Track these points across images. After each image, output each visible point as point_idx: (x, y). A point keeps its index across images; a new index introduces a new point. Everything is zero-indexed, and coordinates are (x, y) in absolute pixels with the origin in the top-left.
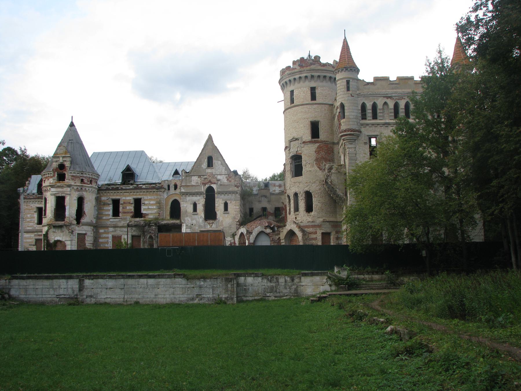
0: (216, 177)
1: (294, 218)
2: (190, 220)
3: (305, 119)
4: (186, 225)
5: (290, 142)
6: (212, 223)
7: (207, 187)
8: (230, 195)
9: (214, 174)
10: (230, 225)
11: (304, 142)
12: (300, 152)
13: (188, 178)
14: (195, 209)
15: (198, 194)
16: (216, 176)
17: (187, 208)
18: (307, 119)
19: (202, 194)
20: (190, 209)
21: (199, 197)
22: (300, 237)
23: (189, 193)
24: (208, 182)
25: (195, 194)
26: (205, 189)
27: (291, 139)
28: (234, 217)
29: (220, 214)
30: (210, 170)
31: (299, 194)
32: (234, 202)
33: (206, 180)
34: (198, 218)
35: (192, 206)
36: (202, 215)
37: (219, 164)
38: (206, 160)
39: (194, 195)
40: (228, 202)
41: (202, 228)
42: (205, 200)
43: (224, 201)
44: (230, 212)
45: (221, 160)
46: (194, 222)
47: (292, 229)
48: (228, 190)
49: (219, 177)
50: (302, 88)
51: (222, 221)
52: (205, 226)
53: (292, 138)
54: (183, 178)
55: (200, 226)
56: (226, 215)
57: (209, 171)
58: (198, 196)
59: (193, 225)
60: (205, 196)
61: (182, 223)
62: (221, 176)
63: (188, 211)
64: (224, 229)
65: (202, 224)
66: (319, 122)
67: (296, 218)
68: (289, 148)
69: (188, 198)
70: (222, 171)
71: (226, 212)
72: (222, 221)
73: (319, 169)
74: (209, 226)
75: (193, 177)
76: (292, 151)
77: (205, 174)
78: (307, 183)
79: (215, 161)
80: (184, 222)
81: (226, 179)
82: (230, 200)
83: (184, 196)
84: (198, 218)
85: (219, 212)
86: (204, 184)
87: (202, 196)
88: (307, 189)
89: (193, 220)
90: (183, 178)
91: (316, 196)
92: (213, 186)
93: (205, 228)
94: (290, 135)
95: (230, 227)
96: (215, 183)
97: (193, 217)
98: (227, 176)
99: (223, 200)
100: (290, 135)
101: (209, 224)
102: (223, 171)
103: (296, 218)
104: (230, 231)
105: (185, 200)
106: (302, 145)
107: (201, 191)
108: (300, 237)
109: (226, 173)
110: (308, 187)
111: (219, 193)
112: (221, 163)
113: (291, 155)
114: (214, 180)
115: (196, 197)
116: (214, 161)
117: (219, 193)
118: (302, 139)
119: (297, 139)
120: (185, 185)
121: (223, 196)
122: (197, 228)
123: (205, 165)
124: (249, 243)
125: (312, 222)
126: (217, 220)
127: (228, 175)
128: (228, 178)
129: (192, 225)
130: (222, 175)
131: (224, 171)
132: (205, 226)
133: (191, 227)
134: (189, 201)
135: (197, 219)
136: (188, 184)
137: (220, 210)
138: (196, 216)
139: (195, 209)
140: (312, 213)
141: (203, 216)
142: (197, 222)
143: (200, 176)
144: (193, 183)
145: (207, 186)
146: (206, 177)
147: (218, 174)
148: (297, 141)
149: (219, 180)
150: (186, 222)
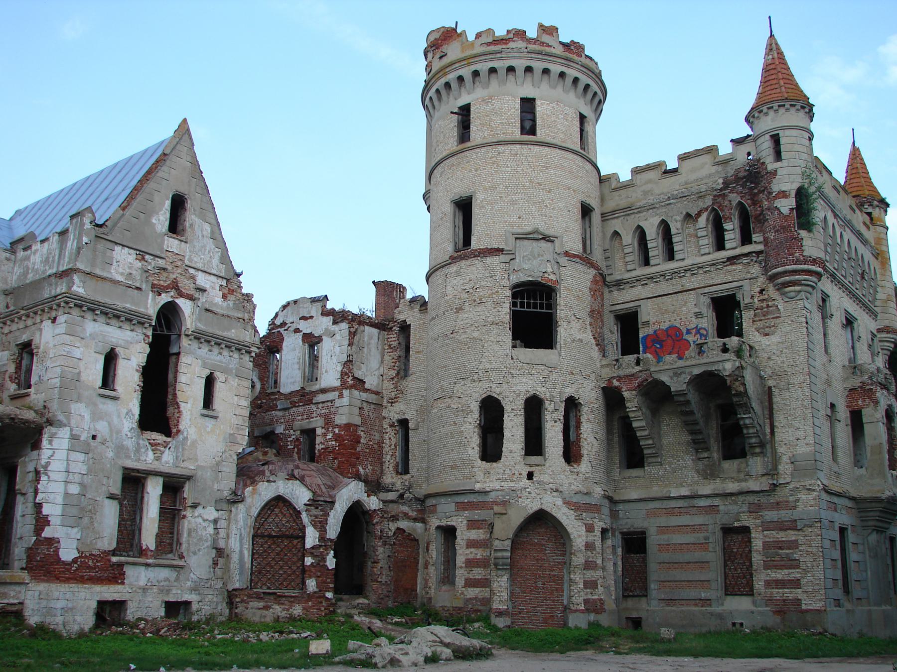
0: (193, 278)
1: (525, 474)
2: (87, 417)
3: (569, 189)
4: (74, 438)
5: (516, 238)
6: (166, 445)
7: (163, 302)
8: (226, 352)
9: (187, 262)
10: (218, 464)
11: (567, 254)
12: (552, 277)
13: (101, 245)
14: (108, 379)
15: (129, 320)
16: (192, 271)
17: (82, 364)
18: (574, 191)
19: (143, 324)
20: (94, 372)
21: (129, 333)
22: (579, 536)
23: (99, 304)
24: (167, 287)
25: (118, 317)
26: (157, 309)
27: (520, 231)
28: (230, 434)
29: (191, 414)
30: (177, 242)
31: (547, 403)
32: (234, 382)
33: (165, 274)
34: (119, 416)
35: (102, 359)
36: (131, 405)
37: (205, 233)
38: (168, 204)
39: (114, 321)
40: (219, 376)
41: (128, 457)
42: (148, 350)
43: (207, 372)
44: (220, 415)
45: (213, 221)
46: (102, 428)
47: (545, 507)
48: (225, 334)
49: (202, 280)
50: (562, 105)
51: (194, 442)
52: (138, 450)
53: (529, 229)
54: (85, 240)
55: (120, 449)
56: (210, 423)
57: (172, 244)
58: (126, 326)
59: (98, 439)
60: (150, 333)
61: (50, 422)
62: (207, 276)
63: (83, 377)
64: (199, 473)
65: (130, 444)
66: (592, 211)
67: (530, 476)
68: (512, 257)
69: (93, 327)
70: (210, 262)
71: (205, 412)
72: (194, 442)
73: (593, 341)
74: (151, 455)
75: (118, 248)
76: (526, 267)
77: (158, 253)
78: (573, 374)
79: (193, 217)
80: (65, 421)
81: (221, 293)
82: (225, 371)
83: (76, 312)
84: (119, 416)
85: (189, 406)
86: (158, 290)
87: (139, 330)
88: (569, 391)
89: (101, 418)
90: (85, 240)
91: (590, 417)
92: (181, 302)
93: (138, 460)
94: (515, 219)
95: (217, 469)
96: (191, 298)
97: (101, 406)
98: (224, 283)
99: (205, 365)
100: (515, 219)
101: (154, 445)
102: (216, 261)
103: (530, 476)
104: (216, 487)
105: (79, 329)
106: (563, 260)
107: (142, 310)
108: (579, 536)
109: (223, 274)
110: (573, 386)
111: (199, 337)
112: (212, 232)
113: (516, 279)
114: (186, 286)
115: (118, 331)
116: (191, 217)
117: (199, 337)
118: (562, 245)
119: (546, 238)
120: (88, 270)
121: (205, 349)
122: (110, 454)
123: (162, 220)
124: (322, 538)
125: (587, 494)
126: (181, 437)
127: (228, 280)
128: (226, 291)
129: (94, 437)
130: (210, 274)
131: (215, 265)
132: (138, 450)
133: (89, 444)
134: (93, 336)
135: (115, 420)
136: (98, 272)
137: (190, 402)
138: (108, 406)
139: (108, 379)
140: (584, 466)
141: (136, 411)
142: (111, 430)
143: (142, 255)
144: (116, 273)
145: (165, 298)
146: (161, 263)
147: (199, 266)
148: (543, 244)
149: (202, 290)
150: (73, 422)
